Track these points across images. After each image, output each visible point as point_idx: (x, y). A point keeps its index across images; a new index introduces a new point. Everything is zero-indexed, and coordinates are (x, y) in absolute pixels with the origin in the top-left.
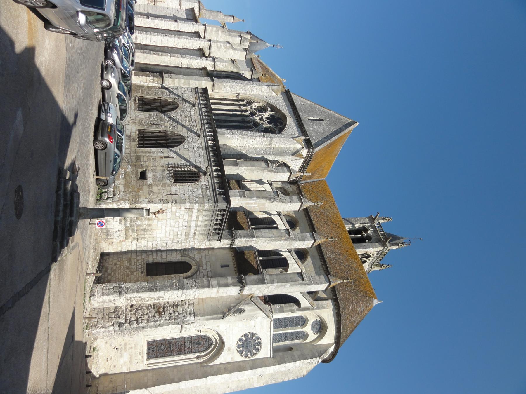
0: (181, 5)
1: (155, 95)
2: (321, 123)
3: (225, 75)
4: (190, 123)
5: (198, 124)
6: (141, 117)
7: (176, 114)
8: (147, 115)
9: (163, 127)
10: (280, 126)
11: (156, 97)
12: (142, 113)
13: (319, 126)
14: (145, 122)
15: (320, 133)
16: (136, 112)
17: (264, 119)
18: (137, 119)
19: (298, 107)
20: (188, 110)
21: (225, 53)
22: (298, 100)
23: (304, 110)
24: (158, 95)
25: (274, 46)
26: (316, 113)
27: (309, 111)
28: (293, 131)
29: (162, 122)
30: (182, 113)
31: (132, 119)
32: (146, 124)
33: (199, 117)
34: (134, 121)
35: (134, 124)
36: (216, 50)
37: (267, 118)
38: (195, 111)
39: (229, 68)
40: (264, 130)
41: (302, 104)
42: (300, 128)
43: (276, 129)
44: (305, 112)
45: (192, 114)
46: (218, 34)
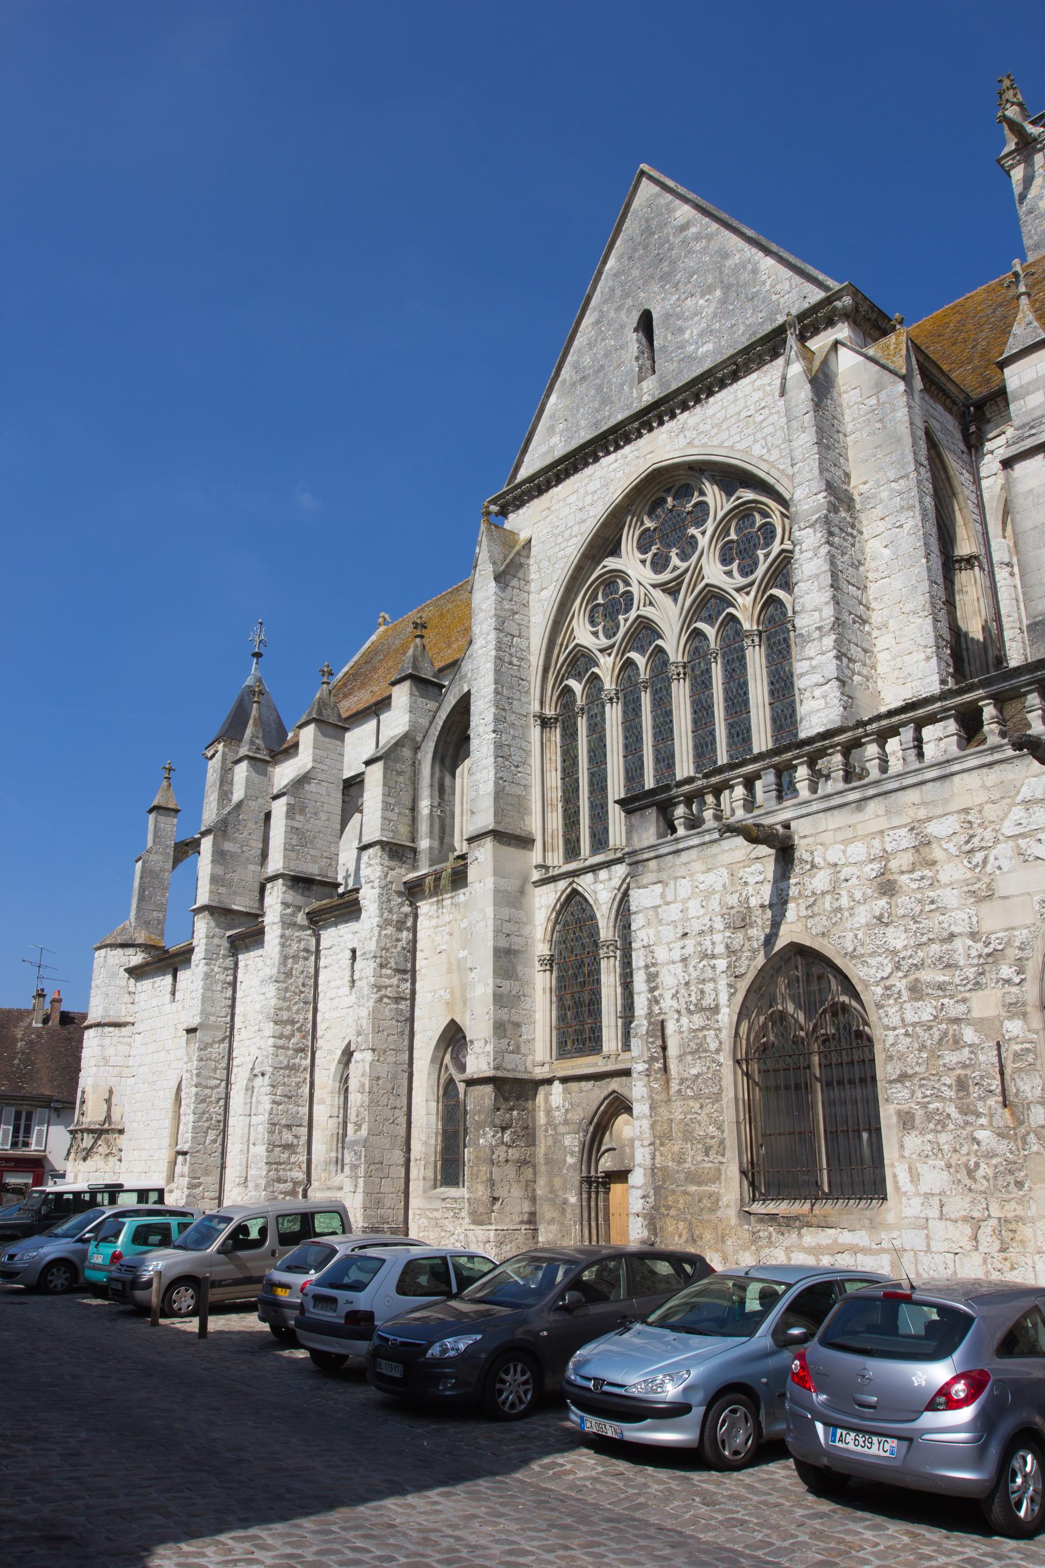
0: (117, 1020)
1: (717, 1097)
2: (667, 316)
3: (432, 797)
4: (937, 853)
5: (945, 802)
6: (934, 1178)
7: (873, 954)
8: (913, 1142)
9: (1014, 1027)
10: (702, 493)
11: (729, 1095)
12: (903, 1177)
13: (686, 319)
14: (990, 1155)
15: (723, 302)
16: (891, 1218)
17: (665, 576)
18: (958, 1205)
19: (585, 435)
20: (820, 881)
21: (323, 816)
22: (543, 449)
23: (598, 411)
24: (717, 1078)
25: (258, 655)
26: (606, 356)
27: (599, 388)
28: (733, 420)
29: (969, 1035)
30: (863, 916)
31: (968, 1245)
32: (1002, 1147)
33: (872, 806)
34: (987, 1230)
35: (1025, 1231)
36: (312, 852)
37: (659, 564)
38: (827, 837)
39: (401, 779)
40: (735, 565)
41: (567, 430)
42: (711, 394)
43: (725, 510)
44: (606, 400)
45: (858, 851)
46: (234, 855)
